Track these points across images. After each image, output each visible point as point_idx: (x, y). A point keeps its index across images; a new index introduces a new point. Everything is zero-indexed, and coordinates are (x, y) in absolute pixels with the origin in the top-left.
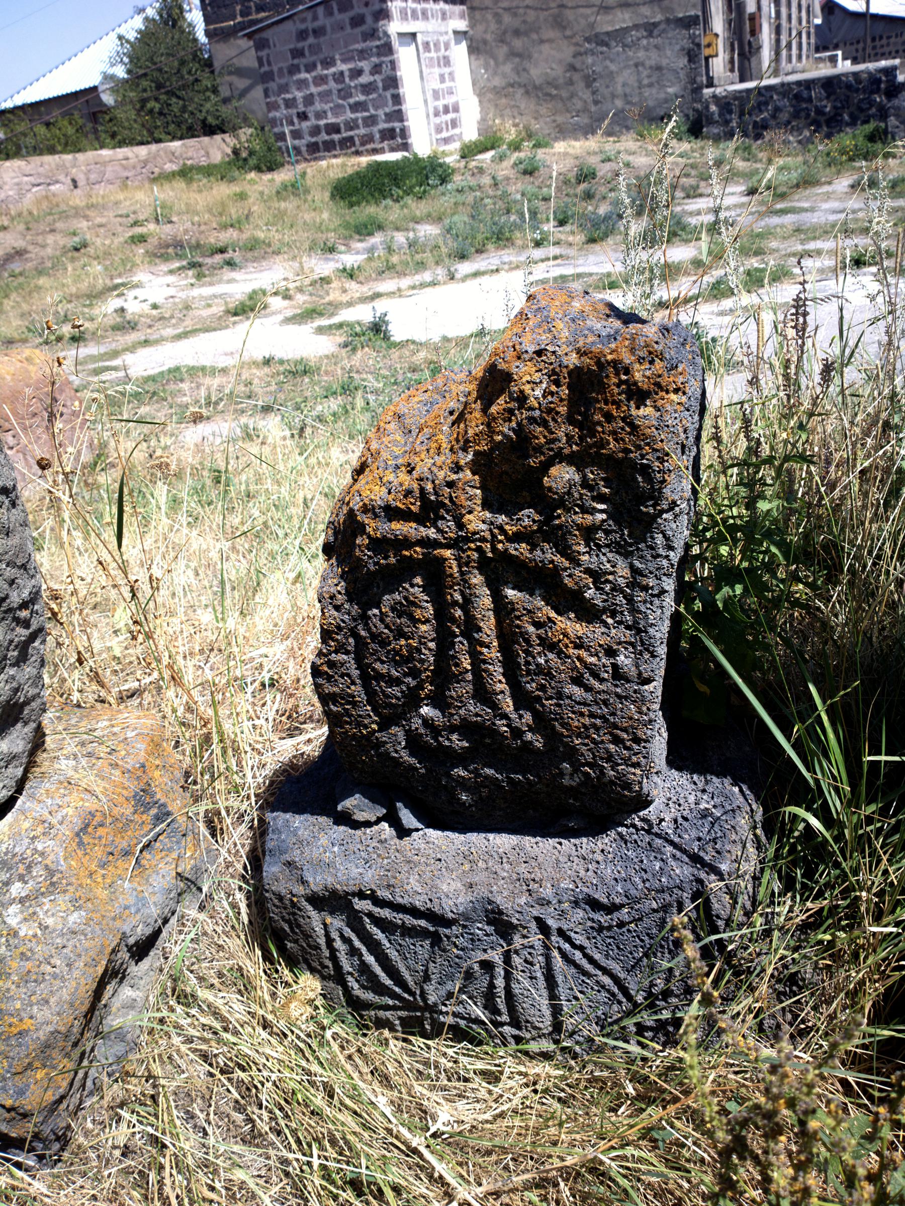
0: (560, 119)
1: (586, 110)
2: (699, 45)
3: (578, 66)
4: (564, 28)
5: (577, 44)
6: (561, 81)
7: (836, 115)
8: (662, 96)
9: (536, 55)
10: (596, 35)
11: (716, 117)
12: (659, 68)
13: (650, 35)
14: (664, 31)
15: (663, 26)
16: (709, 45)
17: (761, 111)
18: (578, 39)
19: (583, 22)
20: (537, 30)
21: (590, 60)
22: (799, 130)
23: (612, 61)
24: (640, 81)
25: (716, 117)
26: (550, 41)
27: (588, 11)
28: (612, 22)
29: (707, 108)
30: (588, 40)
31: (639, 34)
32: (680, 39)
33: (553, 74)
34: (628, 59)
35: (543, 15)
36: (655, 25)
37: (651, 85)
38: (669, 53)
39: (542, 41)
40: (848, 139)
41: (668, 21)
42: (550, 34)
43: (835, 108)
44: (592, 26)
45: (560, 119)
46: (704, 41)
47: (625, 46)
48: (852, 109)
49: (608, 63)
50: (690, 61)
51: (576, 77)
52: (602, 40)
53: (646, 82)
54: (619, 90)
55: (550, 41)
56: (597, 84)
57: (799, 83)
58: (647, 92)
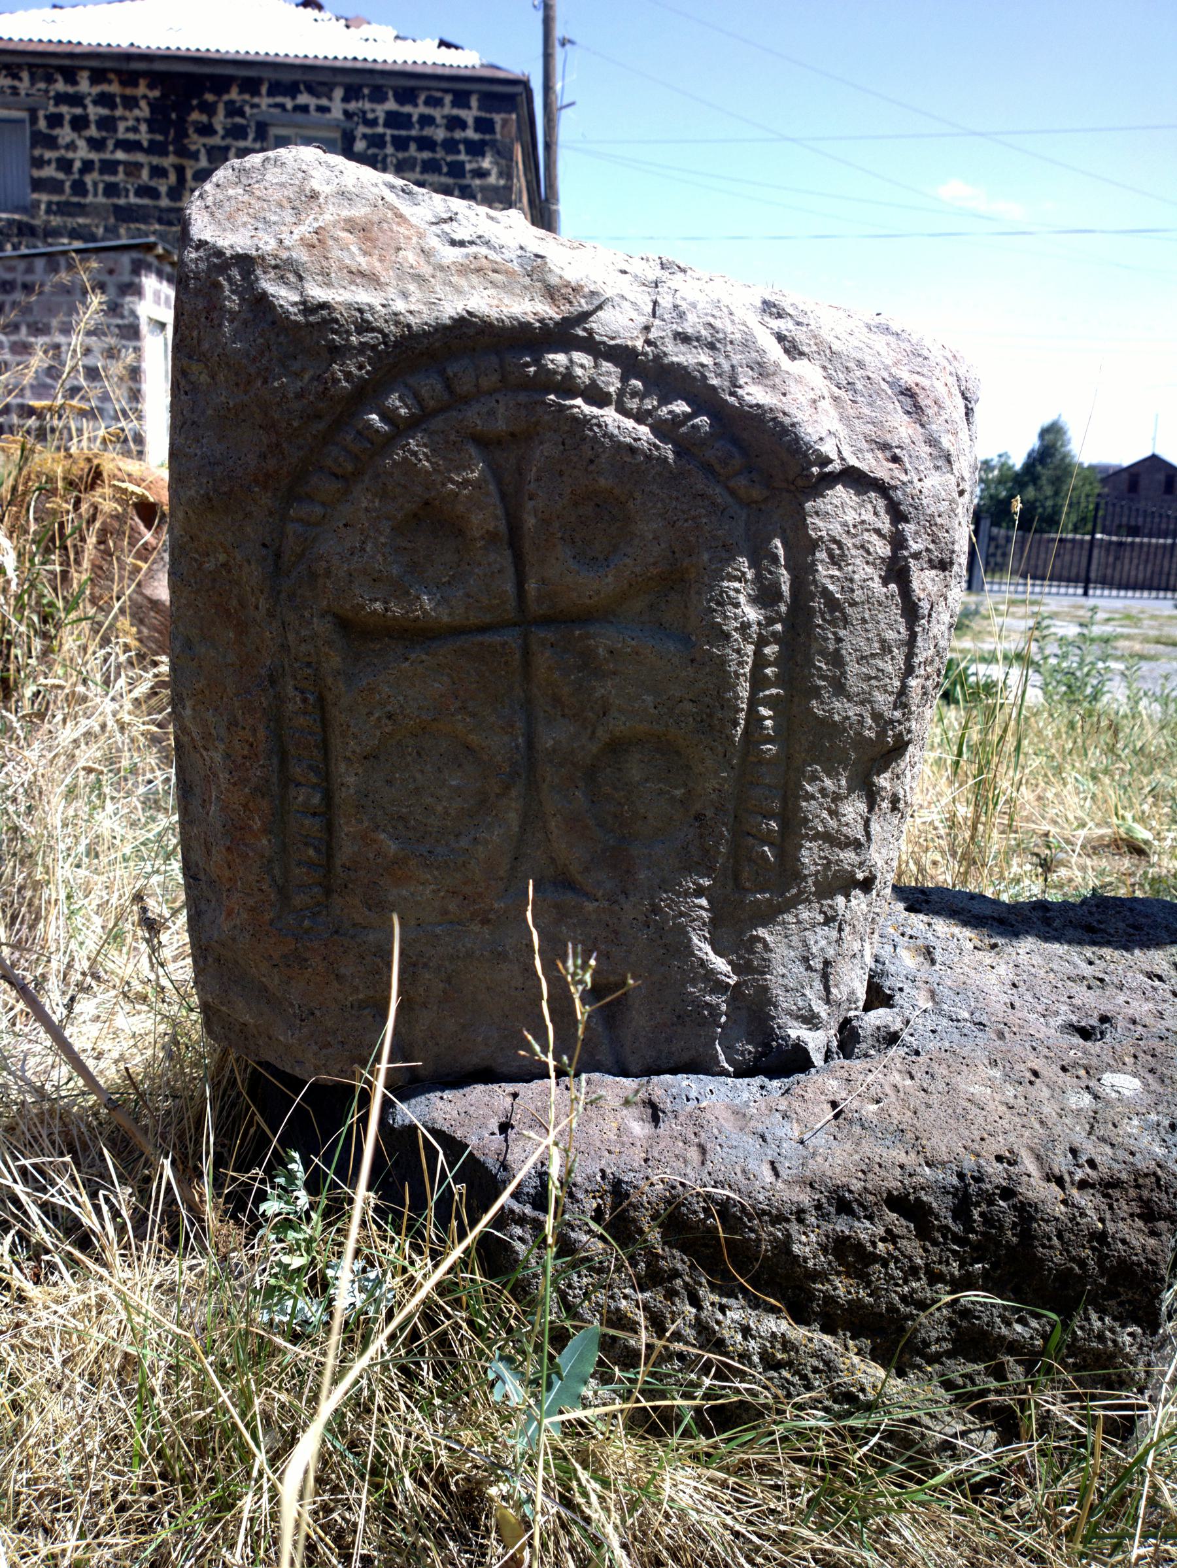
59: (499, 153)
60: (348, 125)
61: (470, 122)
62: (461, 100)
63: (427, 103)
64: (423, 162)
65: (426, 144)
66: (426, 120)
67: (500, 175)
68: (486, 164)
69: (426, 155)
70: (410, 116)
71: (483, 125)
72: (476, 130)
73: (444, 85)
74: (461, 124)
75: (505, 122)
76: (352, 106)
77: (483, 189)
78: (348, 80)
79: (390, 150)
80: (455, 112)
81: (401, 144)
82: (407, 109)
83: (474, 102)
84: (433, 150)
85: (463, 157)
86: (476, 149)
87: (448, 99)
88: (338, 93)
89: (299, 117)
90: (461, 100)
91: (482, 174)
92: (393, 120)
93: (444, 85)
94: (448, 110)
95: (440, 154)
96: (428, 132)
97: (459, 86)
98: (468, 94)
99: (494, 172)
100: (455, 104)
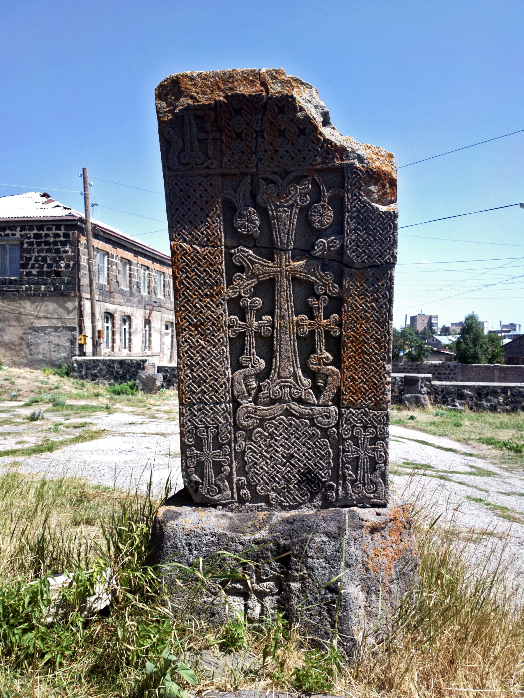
0: (14, 359)
1: (26, 357)
2: (75, 339)
3: (24, 338)
4: (20, 322)
5: (25, 329)
6: (17, 343)
8: (59, 356)
9: (7, 331)
10: (34, 327)
11: (76, 369)
12: (58, 345)
13: (56, 331)
14: (61, 331)
15: (61, 329)
16: (80, 339)
17: (95, 369)
18: (26, 328)
20: (9, 321)
21: (30, 337)
22: (109, 379)
25: (76, 369)
26: (13, 326)
27: (31, 317)
29: (73, 364)
30: (30, 328)
32: (68, 335)
33: (14, 340)
34: (46, 339)
35: (12, 315)
36: (58, 328)
37: (54, 351)
39: (10, 326)
40: (125, 386)
41: (63, 327)
42: (15, 323)
44: (32, 323)
45: (14, 359)
46: (78, 338)
47: (45, 334)
48: (130, 374)
50: (72, 344)
51: (23, 342)
52: (36, 330)
53: (53, 349)
54: (41, 351)
55: (13, 326)
57: (109, 360)
58: (53, 354)
59: (71, 245)
60: (22, 239)
61: (62, 235)
62: (58, 228)
63: (47, 230)
65: (47, 243)
66: (47, 235)
67: (72, 252)
68: (67, 248)
69: (47, 247)
70: (42, 234)
71: (66, 235)
73: (51, 223)
74: (59, 236)
75: (73, 234)
76: (23, 233)
77: (66, 257)
79: (35, 246)
80: (56, 232)
81: (39, 244)
82: (41, 232)
85: (59, 247)
86: (64, 244)
87: (54, 228)
88: (18, 229)
89: (6, 238)
90: (58, 228)
91: (66, 252)
92: (36, 236)
93: (51, 223)
97: (56, 223)
98: (61, 225)
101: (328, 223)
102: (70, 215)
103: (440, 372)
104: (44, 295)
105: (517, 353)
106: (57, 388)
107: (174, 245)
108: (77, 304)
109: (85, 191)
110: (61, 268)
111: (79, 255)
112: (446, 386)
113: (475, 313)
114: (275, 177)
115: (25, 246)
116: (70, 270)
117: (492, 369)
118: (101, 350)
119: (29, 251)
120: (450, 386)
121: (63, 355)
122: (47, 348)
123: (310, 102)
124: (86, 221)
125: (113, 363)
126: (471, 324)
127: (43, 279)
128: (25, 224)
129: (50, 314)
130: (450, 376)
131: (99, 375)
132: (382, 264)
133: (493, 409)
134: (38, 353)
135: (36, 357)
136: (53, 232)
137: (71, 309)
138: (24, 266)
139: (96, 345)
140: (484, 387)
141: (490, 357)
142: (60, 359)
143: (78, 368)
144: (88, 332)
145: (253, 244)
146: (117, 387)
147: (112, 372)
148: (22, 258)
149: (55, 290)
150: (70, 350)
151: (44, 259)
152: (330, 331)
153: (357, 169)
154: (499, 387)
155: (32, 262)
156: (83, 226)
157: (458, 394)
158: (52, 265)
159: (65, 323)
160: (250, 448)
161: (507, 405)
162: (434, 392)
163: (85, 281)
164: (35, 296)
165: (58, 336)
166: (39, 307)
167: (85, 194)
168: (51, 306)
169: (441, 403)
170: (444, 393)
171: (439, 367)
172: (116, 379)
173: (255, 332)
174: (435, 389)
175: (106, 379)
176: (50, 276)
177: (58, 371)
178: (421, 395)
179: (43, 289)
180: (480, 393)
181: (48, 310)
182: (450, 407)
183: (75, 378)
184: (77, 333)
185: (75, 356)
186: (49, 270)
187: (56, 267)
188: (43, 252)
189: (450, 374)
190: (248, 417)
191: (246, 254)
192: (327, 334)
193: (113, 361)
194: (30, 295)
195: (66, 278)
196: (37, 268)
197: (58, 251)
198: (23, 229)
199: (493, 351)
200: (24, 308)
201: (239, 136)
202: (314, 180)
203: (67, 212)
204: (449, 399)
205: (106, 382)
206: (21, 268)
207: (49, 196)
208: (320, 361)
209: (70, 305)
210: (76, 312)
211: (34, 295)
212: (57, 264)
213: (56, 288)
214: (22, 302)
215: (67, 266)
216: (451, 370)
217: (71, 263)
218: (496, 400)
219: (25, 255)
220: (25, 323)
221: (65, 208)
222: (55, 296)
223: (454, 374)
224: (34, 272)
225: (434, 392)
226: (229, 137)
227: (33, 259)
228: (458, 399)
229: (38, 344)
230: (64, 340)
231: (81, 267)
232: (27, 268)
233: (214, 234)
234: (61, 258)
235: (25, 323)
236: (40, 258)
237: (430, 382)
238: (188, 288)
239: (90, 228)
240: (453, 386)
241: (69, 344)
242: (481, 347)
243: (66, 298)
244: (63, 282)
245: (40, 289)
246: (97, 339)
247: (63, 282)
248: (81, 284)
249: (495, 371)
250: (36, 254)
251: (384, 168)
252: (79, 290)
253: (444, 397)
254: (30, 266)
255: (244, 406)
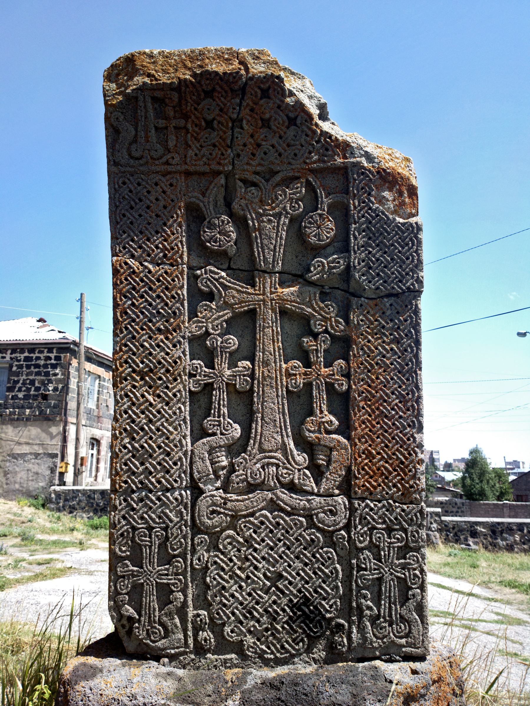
2: (56, 466)
5: (4, 456)
7: (105, 507)
8: (37, 486)
10: (13, 454)
11: (54, 500)
12: (37, 473)
13: (36, 458)
14: (42, 457)
15: (42, 455)
16: (61, 467)
17: (73, 501)
18: (5, 454)
19: (8, 447)
21: (8, 464)
22: (88, 512)
23: (17, 466)
24: (28, 478)
25: (54, 500)
27: (12, 443)
28: (21, 450)
29: (50, 495)
30: (9, 455)
31: (31, 457)
32: (49, 462)
36: (39, 454)
37: (32, 480)
38: (42, 467)
41: (45, 454)
43: (104, 504)
44: (12, 450)
46: (59, 465)
47: (24, 461)
49: (15, 467)
50: (51, 473)
52: (15, 457)
53: (31, 478)
54: (18, 480)
56: (9, 476)
57: (90, 490)
58: (30, 483)
59: (62, 367)
60: (11, 362)
61: (53, 357)
62: (50, 350)
63: (38, 353)
64: (36, 372)
65: (37, 366)
66: (38, 358)
67: (62, 374)
68: (57, 371)
69: (37, 370)
71: (58, 358)
72: (55, 360)
74: (50, 358)
75: (65, 357)
76: (13, 356)
78: (11, 347)
79: (24, 369)
80: (48, 355)
81: (28, 367)
82: (32, 355)
83: (55, 351)
84: (39, 368)
85: (49, 370)
86: (54, 366)
87: (46, 350)
88: (9, 352)
91: (55, 375)
92: (27, 359)
94: (46, 354)
95: (42, 369)
96: (38, 362)
97: (49, 346)
98: (53, 348)
99: (60, 374)
100: (48, 352)
101: (328, 238)
102: (64, 338)
103: (447, 509)
104: (28, 419)
105: (525, 490)
106: (30, 521)
107: (117, 261)
108: (61, 429)
109: (81, 314)
110: (49, 391)
111: (68, 378)
112: (457, 522)
113: (479, 447)
114: (256, 179)
115: (14, 369)
116: (58, 393)
117: (501, 507)
118: (82, 479)
119: (17, 374)
120: (462, 522)
121: (41, 484)
122: (25, 477)
123: (302, 91)
124: (80, 344)
125: (94, 493)
126: (476, 459)
127: (29, 402)
128: (16, 347)
129: (32, 439)
130: (458, 514)
131: (77, 507)
132: (404, 292)
133: (510, 548)
134: (15, 482)
135: (12, 487)
136: (45, 355)
137: (54, 434)
138: (10, 389)
139: (77, 473)
140: (499, 523)
141: (498, 494)
142: (38, 489)
143: (56, 499)
144: (71, 458)
145: (227, 265)
146: (96, 521)
147: (92, 503)
148: (9, 381)
149: (40, 414)
150: (49, 479)
151: (32, 382)
152: (333, 384)
153: (366, 170)
154: (514, 523)
155: (19, 385)
156: (76, 349)
157: (471, 531)
158: (40, 388)
159: (46, 449)
160: (215, 562)
161: (524, 543)
162: (444, 528)
163: (72, 405)
164: (17, 421)
165: (38, 464)
166: (21, 432)
167: (81, 318)
168: (34, 431)
169: (453, 542)
170: (456, 530)
171: (446, 504)
172: (95, 512)
173: (227, 384)
174: (446, 526)
175: (84, 512)
176: (36, 400)
177: (34, 502)
178: (430, 533)
179: (27, 413)
180: (495, 531)
181: (30, 435)
182: (463, 546)
183: (52, 510)
184: (58, 460)
185: (54, 485)
186: (36, 393)
187: (44, 390)
188: (32, 375)
189: (457, 512)
190: (213, 512)
191: (217, 276)
192: (330, 387)
193: (94, 492)
194: (13, 420)
195: (53, 402)
196: (24, 391)
197: (47, 374)
198: (14, 351)
199: (501, 488)
200: (6, 433)
201: (209, 124)
202: (308, 181)
203: (61, 335)
204: (462, 537)
205: (84, 515)
206: (7, 391)
207: (45, 321)
208: (320, 427)
209: (54, 430)
210: (60, 437)
211: (18, 419)
212: (45, 387)
213: (41, 412)
214: (4, 427)
215: (55, 389)
216: (458, 508)
217: (60, 386)
218: (511, 538)
219: (13, 378)
220: (5, 449)
221: (60, 332)
222: (39, 420)
223: (462, 512)
224: (21, 395)
225: (444, 528)
226: (196, 126)
227: (21, 382)
228: (472, 537)
229: (16, 473)
230: (43, 468)
231: (70, 390)
232: (13, 391)
233: (173, 249)
234: (50, 381)
235: (5, 449)
236: (28, 382)
237: (440, 517)
238: (134, 320)
239: (83, 351)
240: (465, 522)
241: (48, 472)
242: (488, 482)
243: (50, 423)
244: (49, 406)
245: (24, 413)
246: (79, 466)
247: (49, 406)
248: (69, 407)
249: (505, 509)
250: (24, 377)
251: (400, 171)
252: (65, 415)
253: (456, 535)
254: (17, 389)
255: (208, 494)
